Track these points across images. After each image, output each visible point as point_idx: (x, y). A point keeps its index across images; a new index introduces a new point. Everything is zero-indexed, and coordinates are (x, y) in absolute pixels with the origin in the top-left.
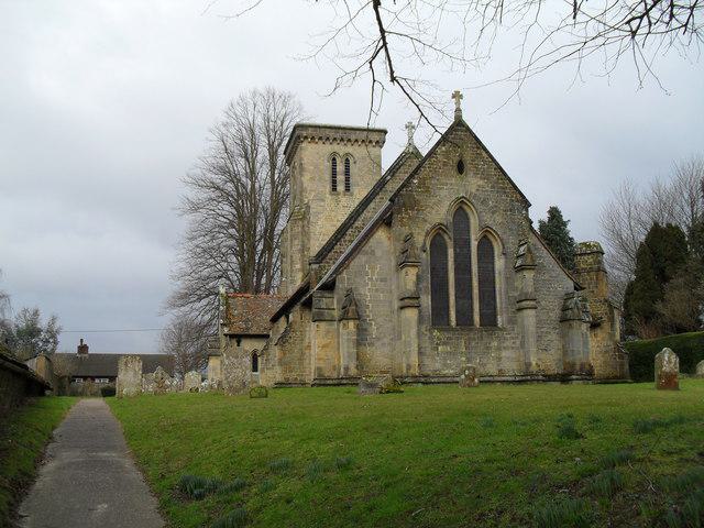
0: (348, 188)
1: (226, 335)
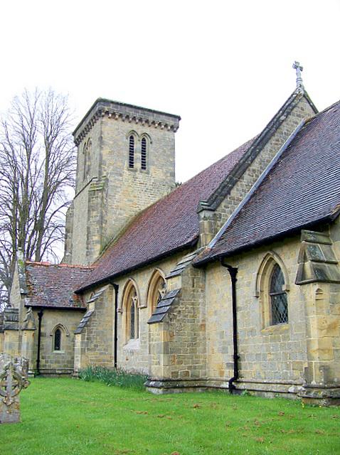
0: (144, 167)
1: (27, 307)
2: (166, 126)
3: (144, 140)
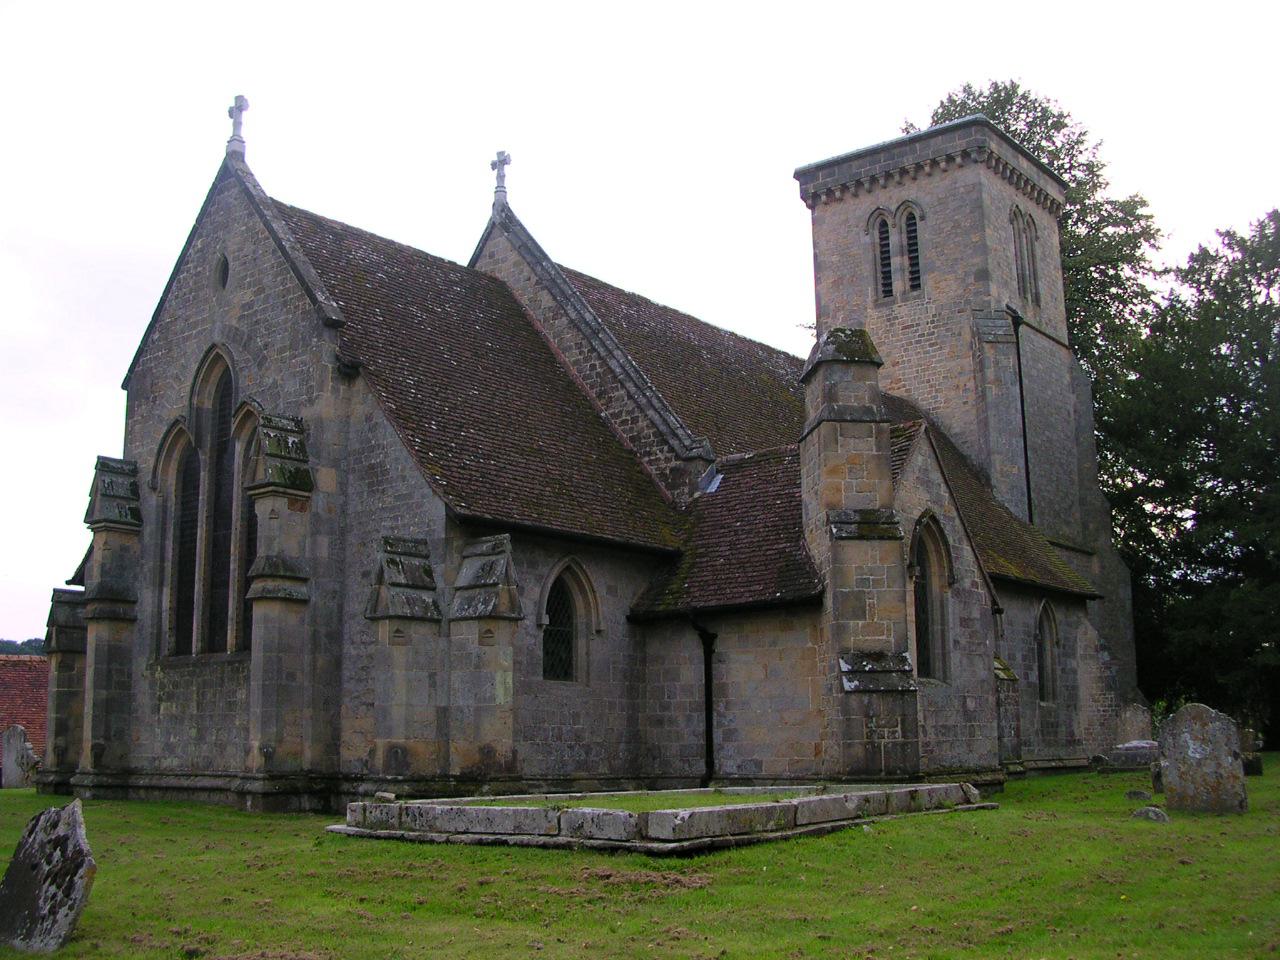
3: (911, 217)
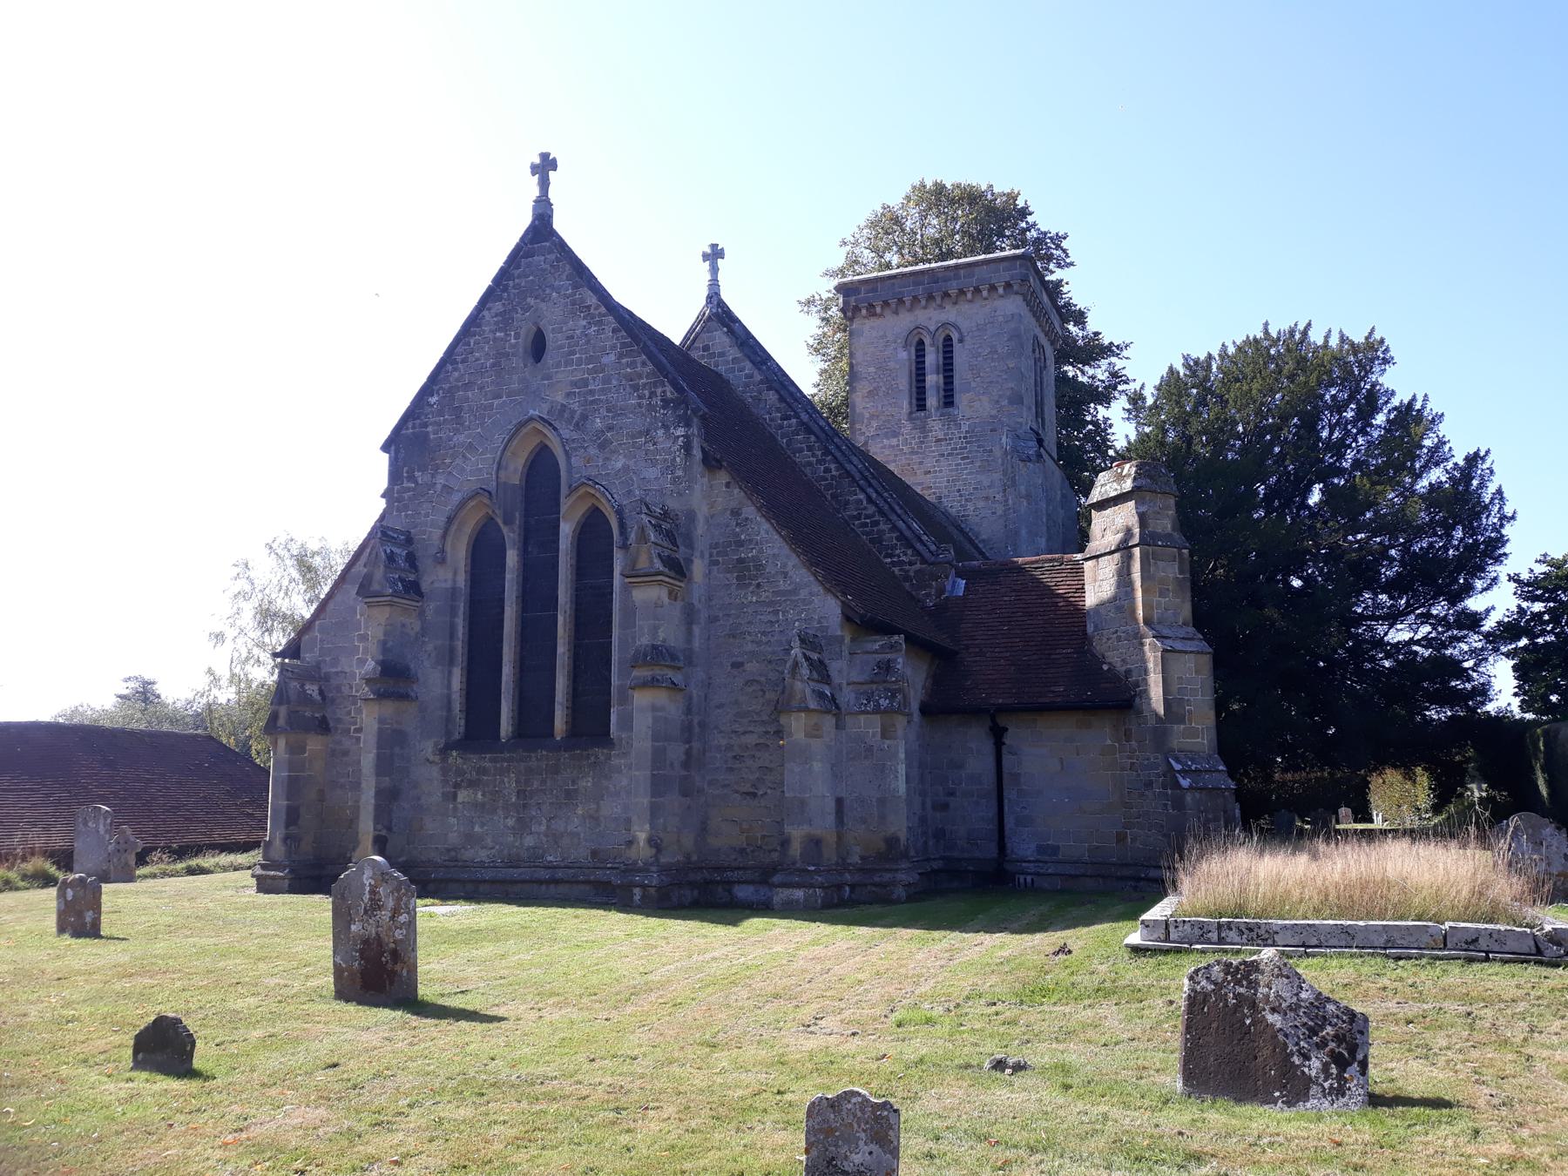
2: (993, 288)
3: (948, 339)
